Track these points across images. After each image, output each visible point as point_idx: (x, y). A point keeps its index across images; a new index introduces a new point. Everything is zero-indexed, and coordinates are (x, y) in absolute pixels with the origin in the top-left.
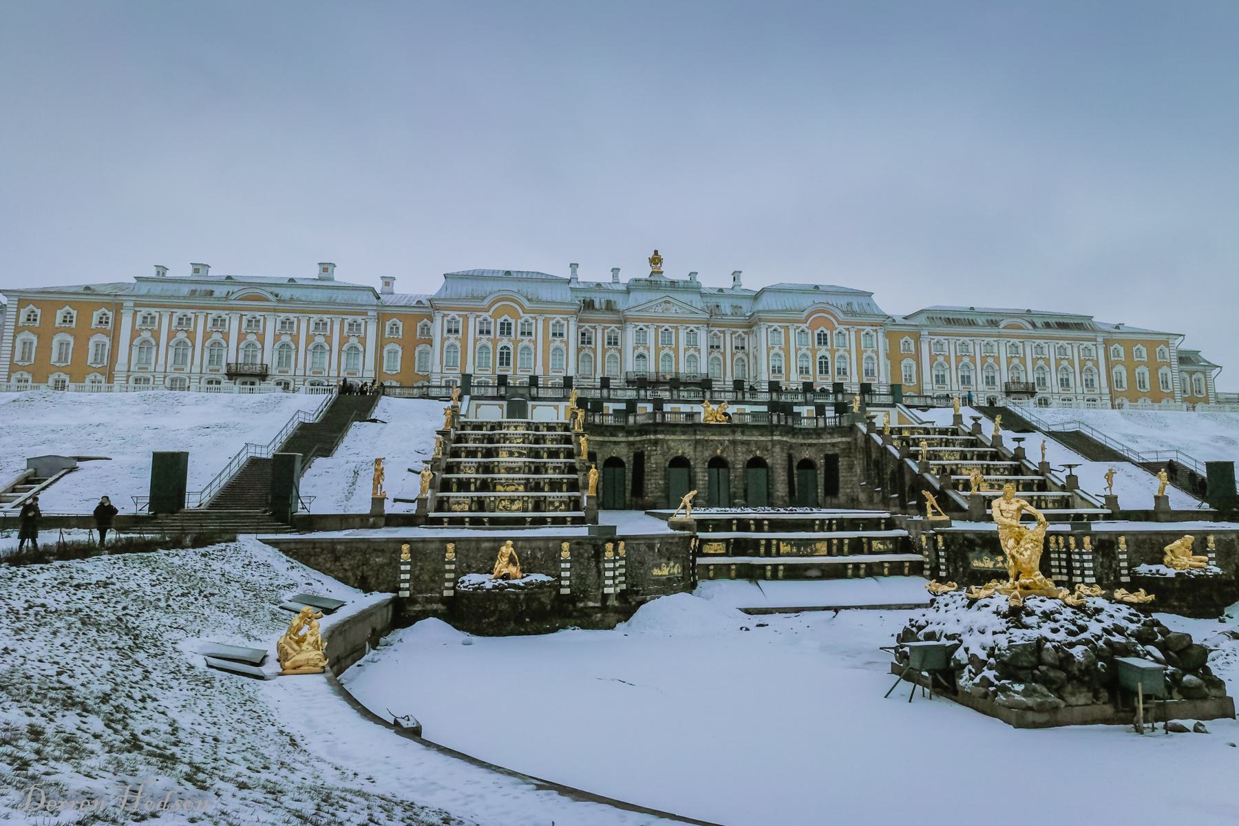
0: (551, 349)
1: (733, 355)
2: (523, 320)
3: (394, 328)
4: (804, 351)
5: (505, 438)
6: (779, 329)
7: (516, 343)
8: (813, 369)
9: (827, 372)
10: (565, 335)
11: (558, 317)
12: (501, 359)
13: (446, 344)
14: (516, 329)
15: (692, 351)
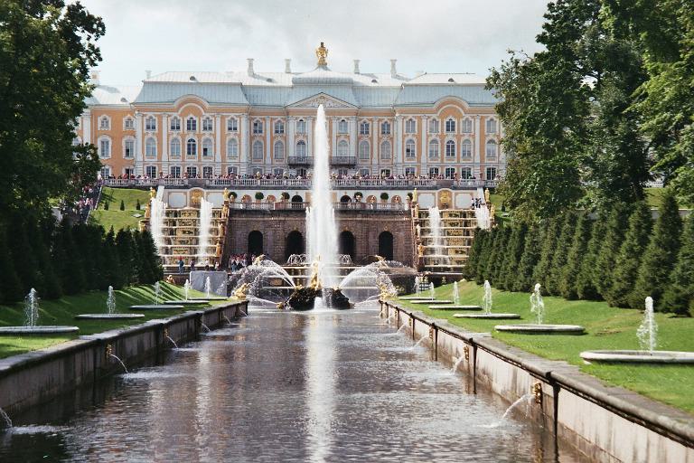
0: (227, 142)
1: (379, 139)
2: (205, 118)
3: (105, 121)
4: (434, 137)
5: (182, 222)
6: (414, 119)
7: (199, 136)
8: (441, 150)
9: (453, 154)
10: (238, 129)
11: (232, 115)
12: (189, 149)
13: (146, 138)
14: (200, 126)
15: (342, 138)
